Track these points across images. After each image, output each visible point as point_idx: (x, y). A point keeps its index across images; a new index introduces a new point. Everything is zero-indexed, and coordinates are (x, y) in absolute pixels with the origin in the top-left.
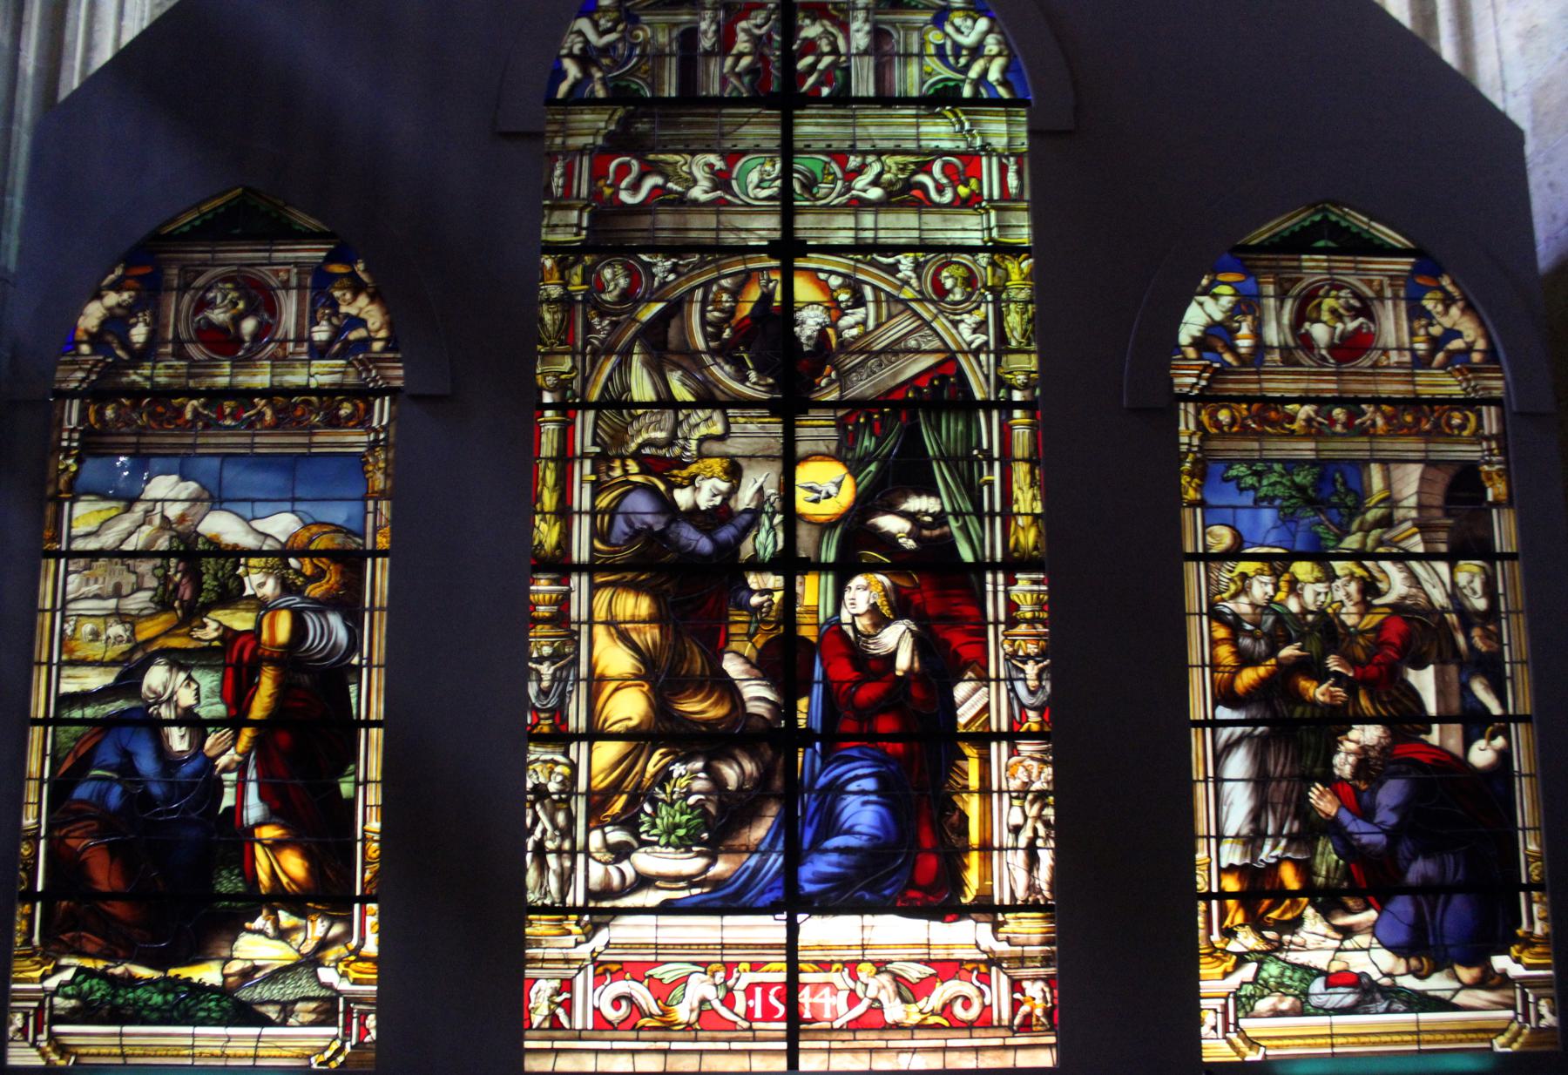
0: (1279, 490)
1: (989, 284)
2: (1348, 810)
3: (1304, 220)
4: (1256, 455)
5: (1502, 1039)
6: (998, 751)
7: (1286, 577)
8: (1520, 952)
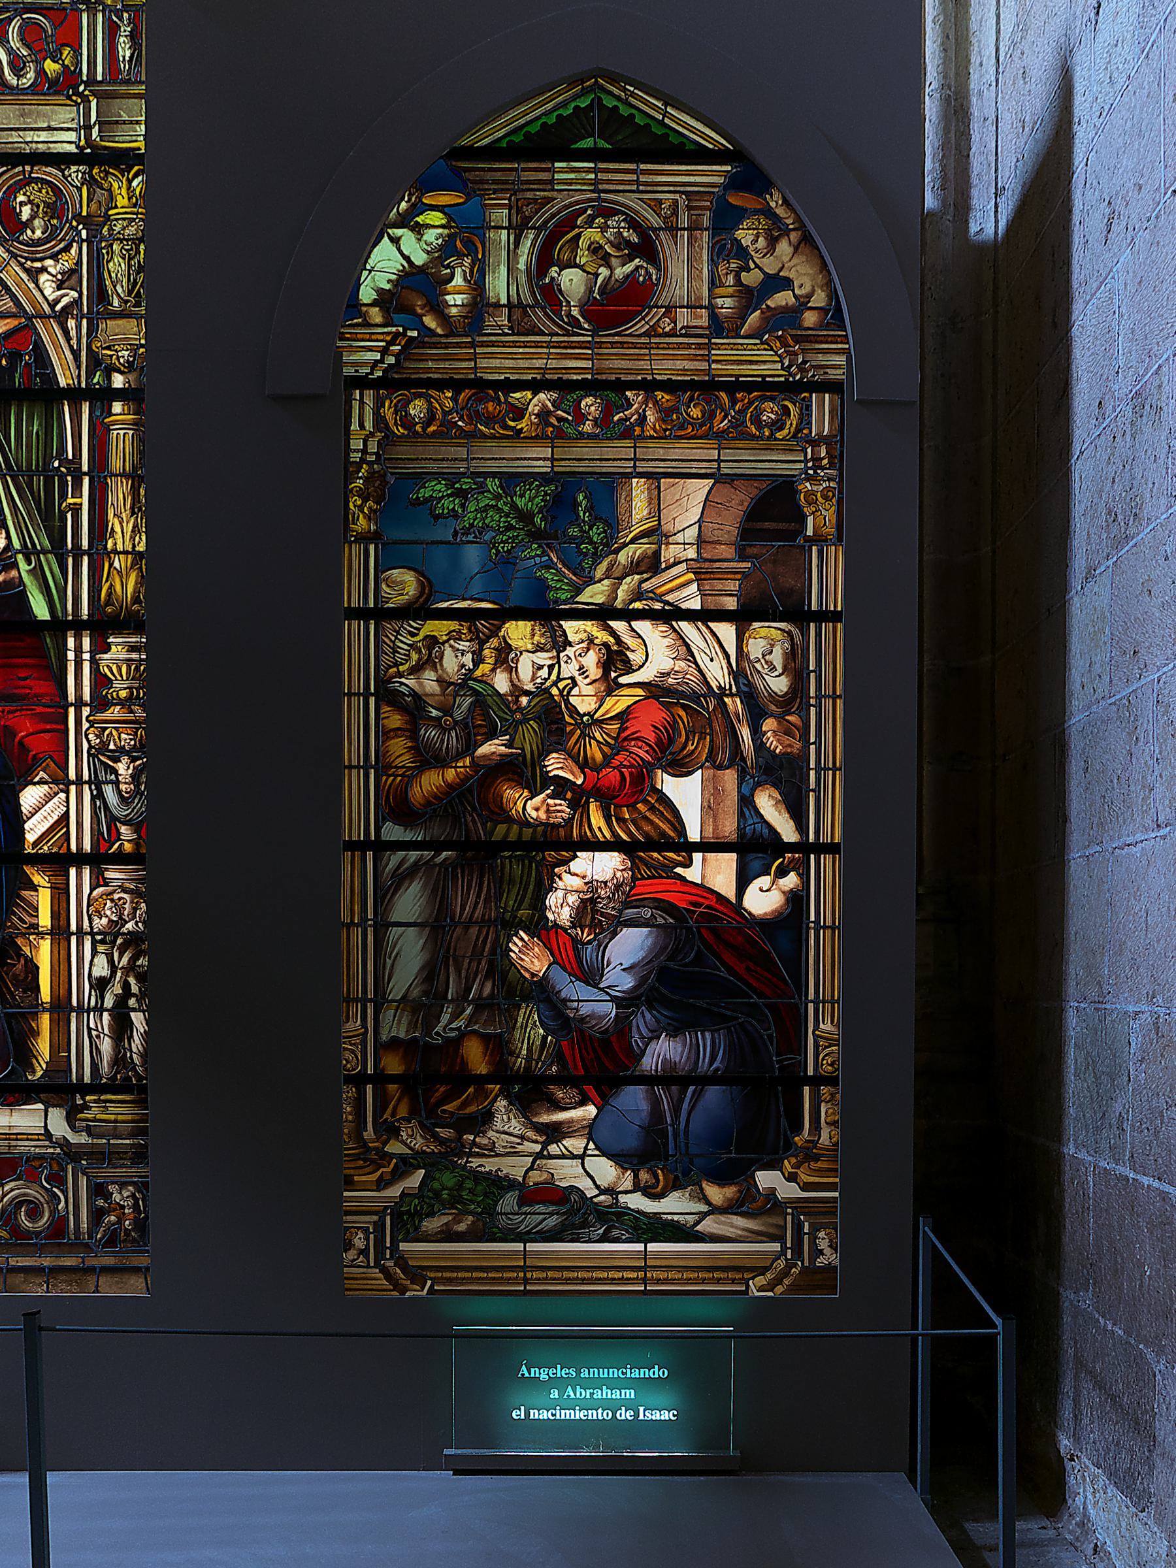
0: (493, 518)
1: (84, 213)
2: (564, 969)
3: (564, 105)
4: (462, 467)
5: (761, 1280)
6: (79, 880)
7: (494, 642)
8: (797, 1166)
